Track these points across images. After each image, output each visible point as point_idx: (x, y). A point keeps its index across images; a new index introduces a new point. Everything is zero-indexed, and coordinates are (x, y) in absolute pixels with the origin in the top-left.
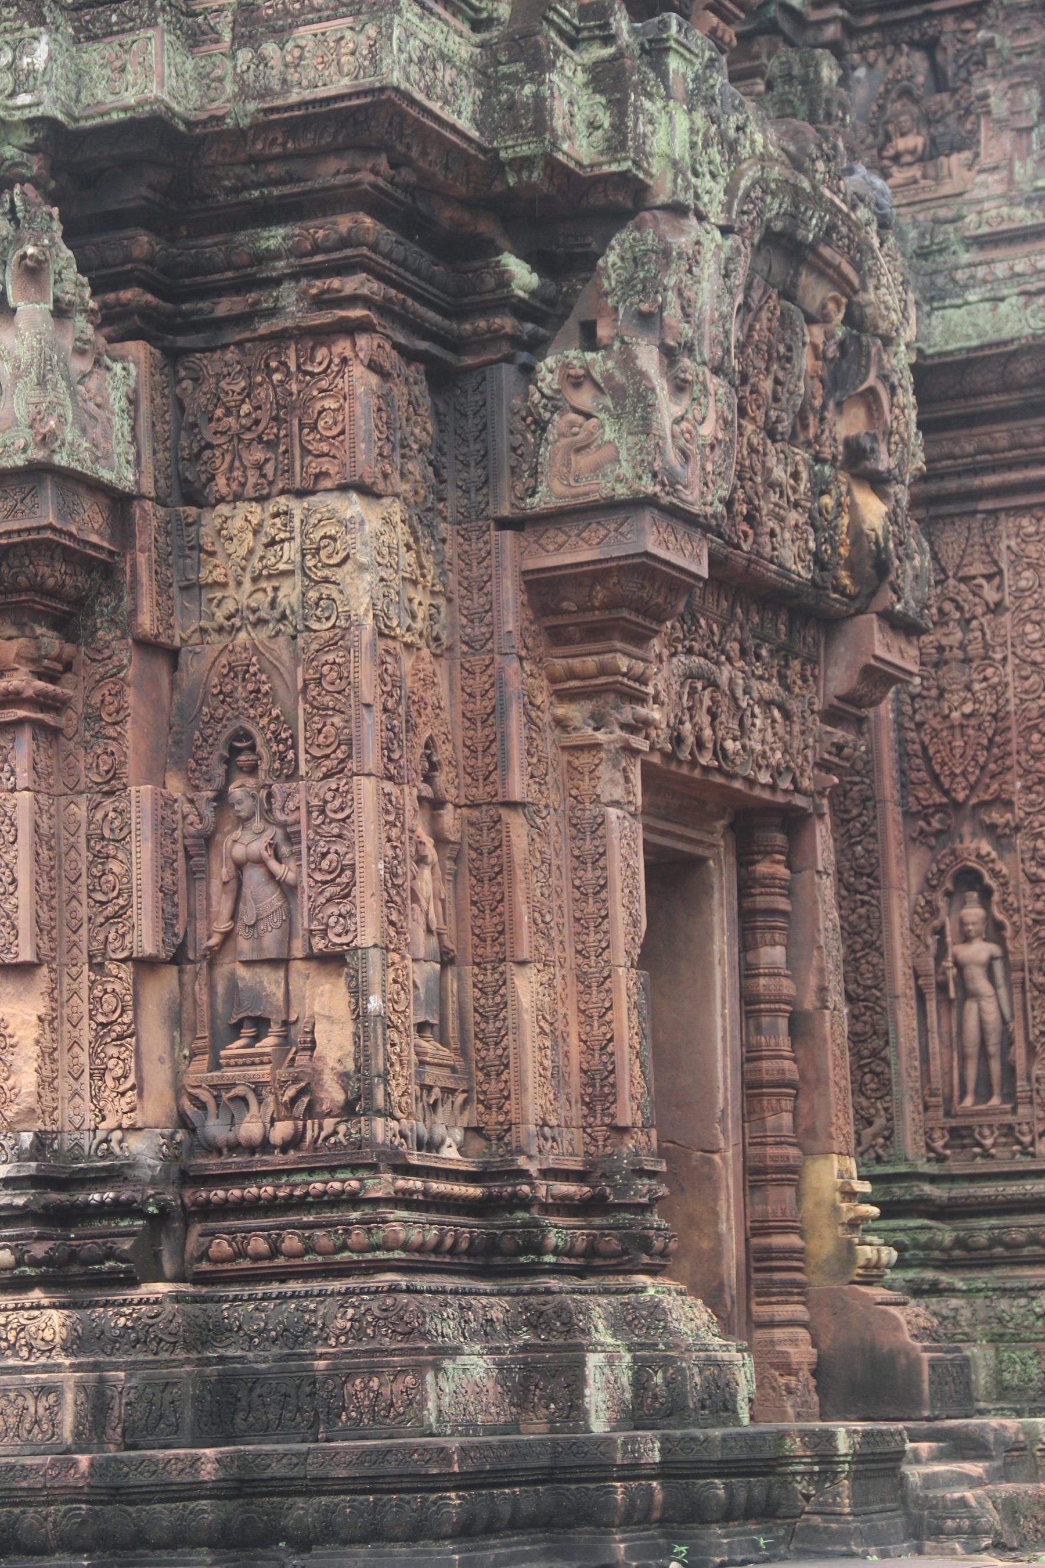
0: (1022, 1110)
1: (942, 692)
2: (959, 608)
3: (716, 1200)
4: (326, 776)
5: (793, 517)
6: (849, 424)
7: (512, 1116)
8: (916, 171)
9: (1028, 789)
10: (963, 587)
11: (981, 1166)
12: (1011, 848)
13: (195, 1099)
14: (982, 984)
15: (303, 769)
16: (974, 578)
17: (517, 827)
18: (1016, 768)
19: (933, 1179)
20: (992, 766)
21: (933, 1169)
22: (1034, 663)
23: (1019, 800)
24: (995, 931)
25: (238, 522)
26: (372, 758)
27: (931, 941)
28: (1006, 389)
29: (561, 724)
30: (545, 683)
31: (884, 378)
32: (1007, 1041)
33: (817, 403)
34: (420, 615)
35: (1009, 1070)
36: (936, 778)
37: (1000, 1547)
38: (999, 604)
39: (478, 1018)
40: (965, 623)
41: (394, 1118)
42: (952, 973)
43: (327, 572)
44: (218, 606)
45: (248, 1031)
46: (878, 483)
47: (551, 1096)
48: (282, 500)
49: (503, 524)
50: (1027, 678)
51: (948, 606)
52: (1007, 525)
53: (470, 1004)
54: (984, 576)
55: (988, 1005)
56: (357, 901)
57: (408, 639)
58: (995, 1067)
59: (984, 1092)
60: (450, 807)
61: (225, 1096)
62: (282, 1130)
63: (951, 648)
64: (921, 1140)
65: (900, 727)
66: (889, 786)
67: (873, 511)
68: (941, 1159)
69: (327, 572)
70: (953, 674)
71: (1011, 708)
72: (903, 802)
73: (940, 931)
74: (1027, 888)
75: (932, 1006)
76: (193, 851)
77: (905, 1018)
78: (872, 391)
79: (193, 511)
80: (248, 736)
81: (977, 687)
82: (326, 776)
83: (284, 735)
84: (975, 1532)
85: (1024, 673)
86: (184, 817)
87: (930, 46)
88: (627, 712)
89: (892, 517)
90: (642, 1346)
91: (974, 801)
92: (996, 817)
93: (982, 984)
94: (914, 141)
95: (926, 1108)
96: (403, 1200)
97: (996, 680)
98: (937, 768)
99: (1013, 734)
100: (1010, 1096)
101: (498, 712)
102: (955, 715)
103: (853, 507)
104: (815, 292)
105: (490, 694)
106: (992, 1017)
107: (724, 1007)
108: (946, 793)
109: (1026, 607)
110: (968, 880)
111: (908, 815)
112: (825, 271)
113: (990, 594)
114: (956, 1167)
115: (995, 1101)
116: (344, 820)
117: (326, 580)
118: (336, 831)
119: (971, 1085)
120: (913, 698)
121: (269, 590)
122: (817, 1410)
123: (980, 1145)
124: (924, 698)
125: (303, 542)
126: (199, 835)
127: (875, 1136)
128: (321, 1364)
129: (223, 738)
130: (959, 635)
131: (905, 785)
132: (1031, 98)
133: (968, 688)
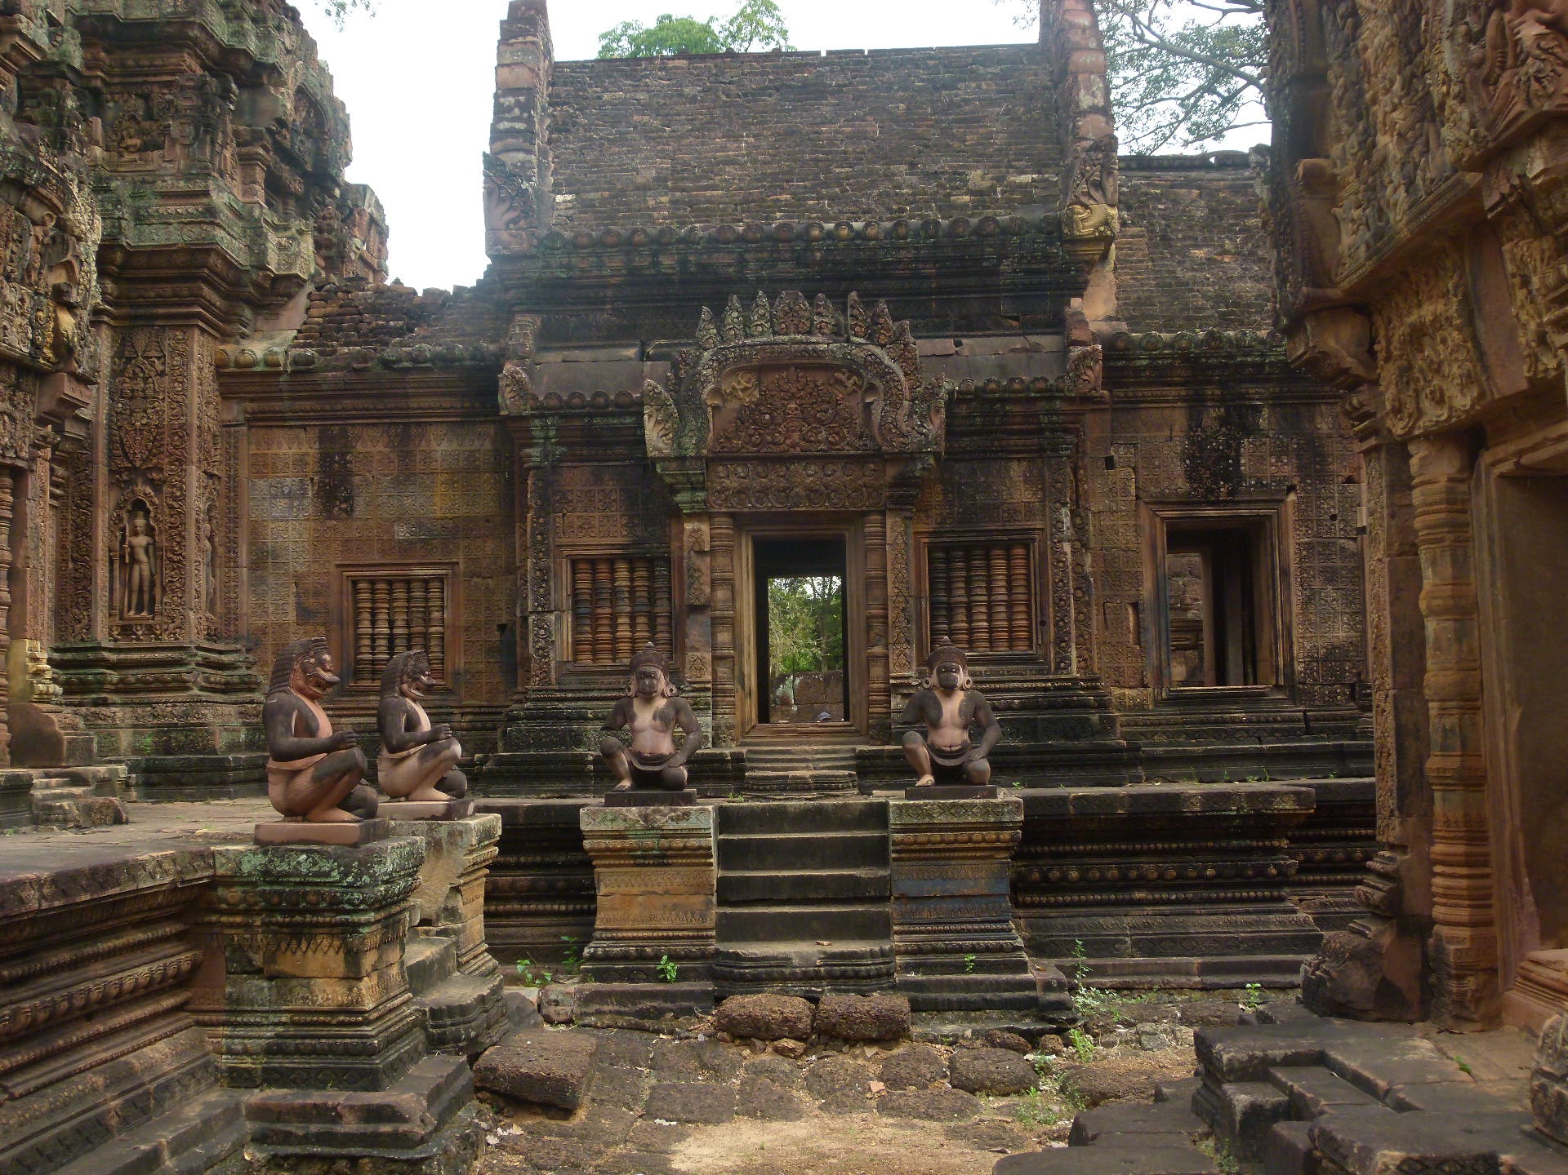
0: (158, 618)
1: (132, 412)
5: (18, 320)
6: (58, 278)
8: (136, 156)
9: (171, 463)
11: (135, 644)
12: (161, 491)
14: (142, 556)
19: (110, 650)
21: (111, 645)
23: (167, 468)
24: (150, 531)
28: (170, 268)
31: (77, 257)
32: (152, 585)
33: (37, 265)
35: (152, 599)
36: (126, 454)
37: (78, 827)
40: (145, 380)
46: (71, 308)
52: (169, 333)
55: (144, 568)
58: (146, 597)
59: (139, 609)
64: (106, 631)
65: (109, 427)
66: (101, 455)
67: (67, 321)
68: (116, 640)
70: (139, 403)
72: (109, 465)
73: (123, 530)
74: (167, 510)
75: (117, 566)
77: (101, 573)
78: (69, 262)
84: (66, 821)
87: (146, 98)
89: (78, 326)
92: (155, 475)
93: (142, 556)
94: (137, 142)
99: (165, 436)
100: (151, 611)
103: (56, 320)
104: (39, 212)
106: (146, 573)
110: (139, 506)
111: (111, 472)
112: (42, 200)
113: (160, 367)
114: (122, 644)
115: (144, 614)
131: (111, 457)
132: (190, 129)
133: (145, 411)
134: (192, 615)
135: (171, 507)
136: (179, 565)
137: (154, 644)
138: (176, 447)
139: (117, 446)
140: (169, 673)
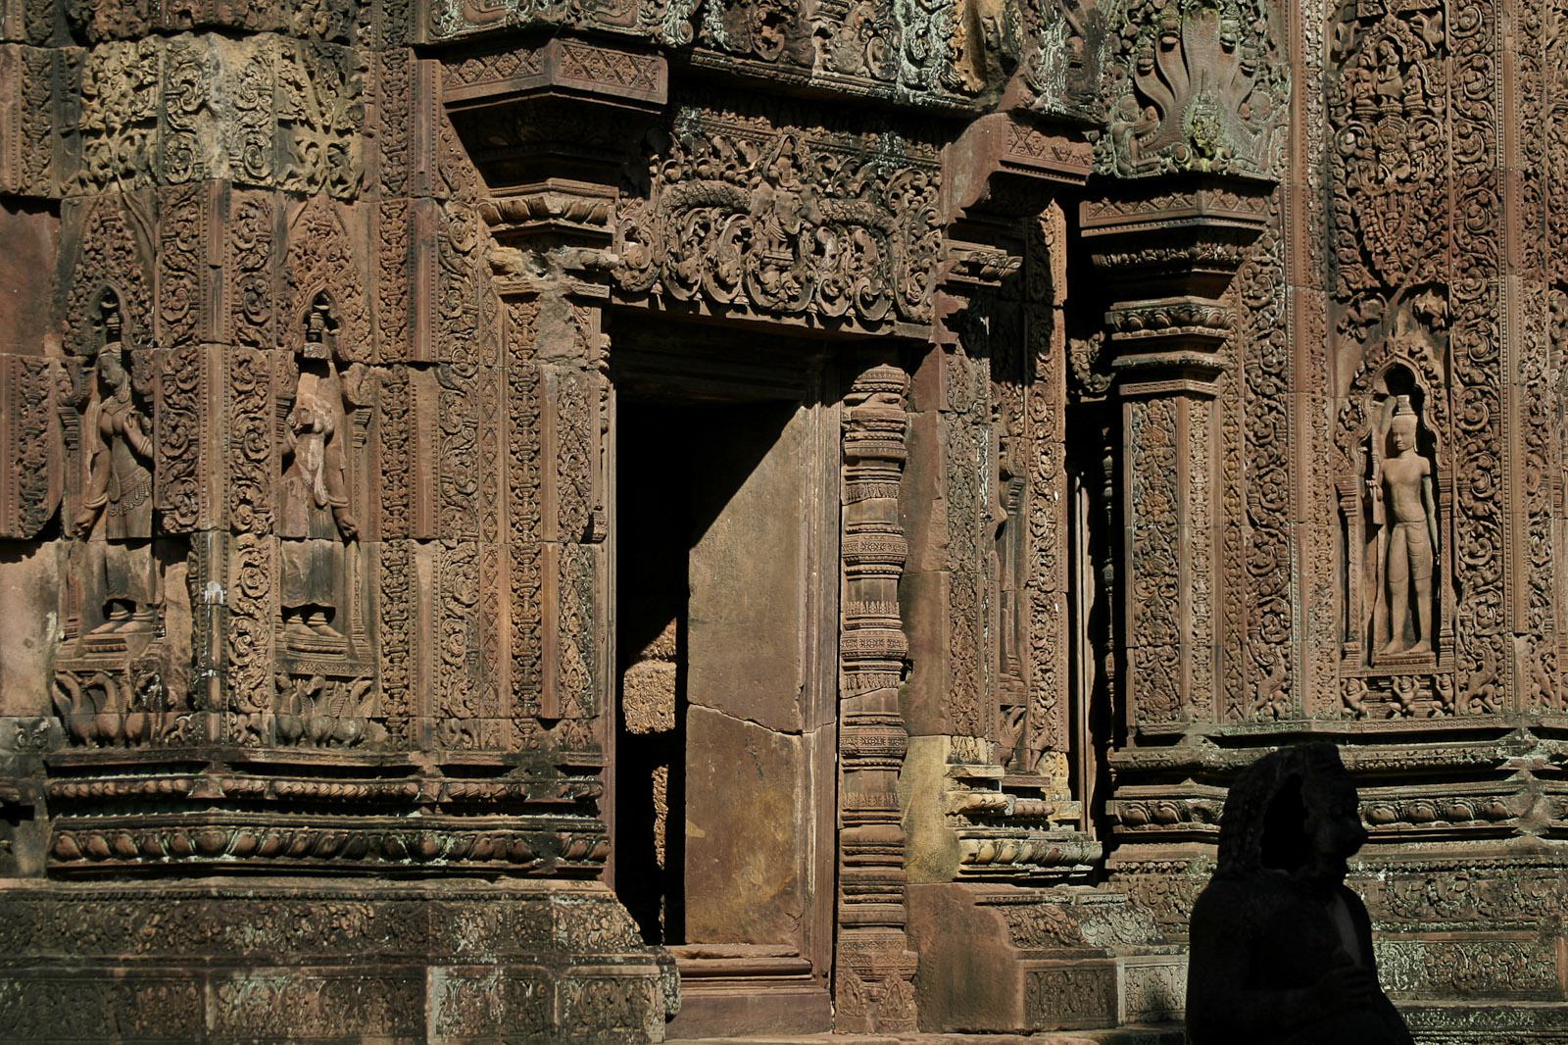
0: (1446, 658)
2: (1398, 50)
3: (793, 787)
4: (177, 343)
7: (410, 708)
10: (1403, 24)
11: (1399, 724)
13: (61, 686)
15: (158, 333)
16: (1413, 13)
17: (423, 387)
18: (1453, 245)
20: (1428, 243)
22: (1475, 118)
24: (1425, 443)
25: (111, 64)
26: (222, 325)
27: (1358, 454)
29: (499, 270)
30: (482, 224)
34: (310, 158)
36: (1366, 256)
38: (1441, 45)
39: (385, 599)
41: (236, 711)
42: (1377, 492)
43: (186, 120)
44: (94, 154)
45: (119, 613)
47: (463, 685)
48: (151, 40)
49: (423, 52)
50: (1466, 137)
51: (1387, 48)
53: (378, 583)
54: (1425, 12)
56: (201, 478)
57: (291, 185)
60: (356, 366)
61: (88, 682)
62: (135, 722)
63: (1388, 97)
68: (1360, 715)
69: (186, 120)
71: (1449, 172)
72: (1330, 286)
76: (67, 419)
79: (78, 50)
80: (111, 297)
81: (1414, 146)
82: (177, 343)
83: (142, 298)
85: (1464, 131)
86: (58, 383)
88: (569, 255)
90: (519, 959)
91: (1407, 284)
92: (1429, 302)
93: (1410, 506)
95: (1344, 654)
96: (233, 800)
97: (1433, 138)
98: (1370, 246)
101: (409, 262)
102: (1390, 179)
105: (404, 240)
107: (810, 569)
108: (1377, 275)
109: (1468, 50)
110: (1400, 380)
116: (191, 391)
117: (184, 129)
118: (184, 403)
119: (1398, 629)
120: (1345, 160)
121: (137, 138)
122: (914, 1019)
123: (1397, 698)
124: (1358, 158)
125: (165, 86)
126: (69, 403)
127: (1273, 688)
128: (120, 970)
129: (92, 297)
130: (1399, 81)
134: (1520, 644)
135: (1470, 384)
136: (1487, 524)
137: (1442, 722)
138: (1472, 231)
139: (1343, 237)
140: (1462, 797)
